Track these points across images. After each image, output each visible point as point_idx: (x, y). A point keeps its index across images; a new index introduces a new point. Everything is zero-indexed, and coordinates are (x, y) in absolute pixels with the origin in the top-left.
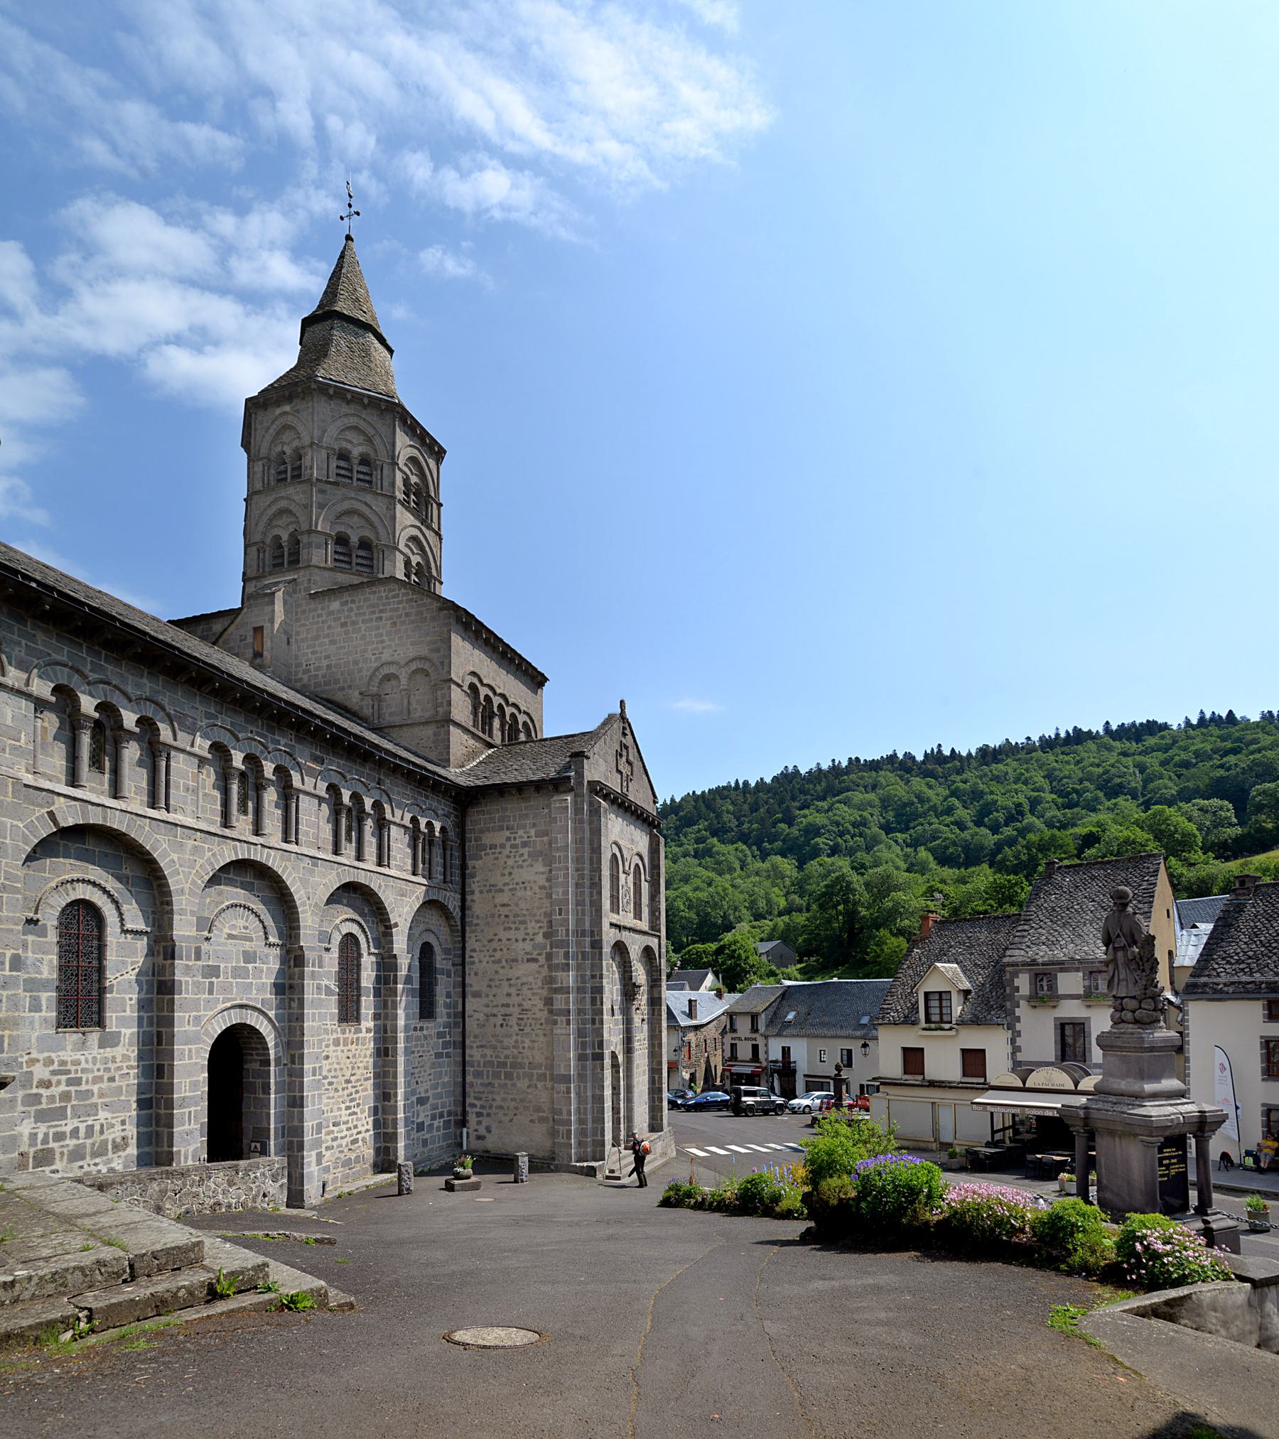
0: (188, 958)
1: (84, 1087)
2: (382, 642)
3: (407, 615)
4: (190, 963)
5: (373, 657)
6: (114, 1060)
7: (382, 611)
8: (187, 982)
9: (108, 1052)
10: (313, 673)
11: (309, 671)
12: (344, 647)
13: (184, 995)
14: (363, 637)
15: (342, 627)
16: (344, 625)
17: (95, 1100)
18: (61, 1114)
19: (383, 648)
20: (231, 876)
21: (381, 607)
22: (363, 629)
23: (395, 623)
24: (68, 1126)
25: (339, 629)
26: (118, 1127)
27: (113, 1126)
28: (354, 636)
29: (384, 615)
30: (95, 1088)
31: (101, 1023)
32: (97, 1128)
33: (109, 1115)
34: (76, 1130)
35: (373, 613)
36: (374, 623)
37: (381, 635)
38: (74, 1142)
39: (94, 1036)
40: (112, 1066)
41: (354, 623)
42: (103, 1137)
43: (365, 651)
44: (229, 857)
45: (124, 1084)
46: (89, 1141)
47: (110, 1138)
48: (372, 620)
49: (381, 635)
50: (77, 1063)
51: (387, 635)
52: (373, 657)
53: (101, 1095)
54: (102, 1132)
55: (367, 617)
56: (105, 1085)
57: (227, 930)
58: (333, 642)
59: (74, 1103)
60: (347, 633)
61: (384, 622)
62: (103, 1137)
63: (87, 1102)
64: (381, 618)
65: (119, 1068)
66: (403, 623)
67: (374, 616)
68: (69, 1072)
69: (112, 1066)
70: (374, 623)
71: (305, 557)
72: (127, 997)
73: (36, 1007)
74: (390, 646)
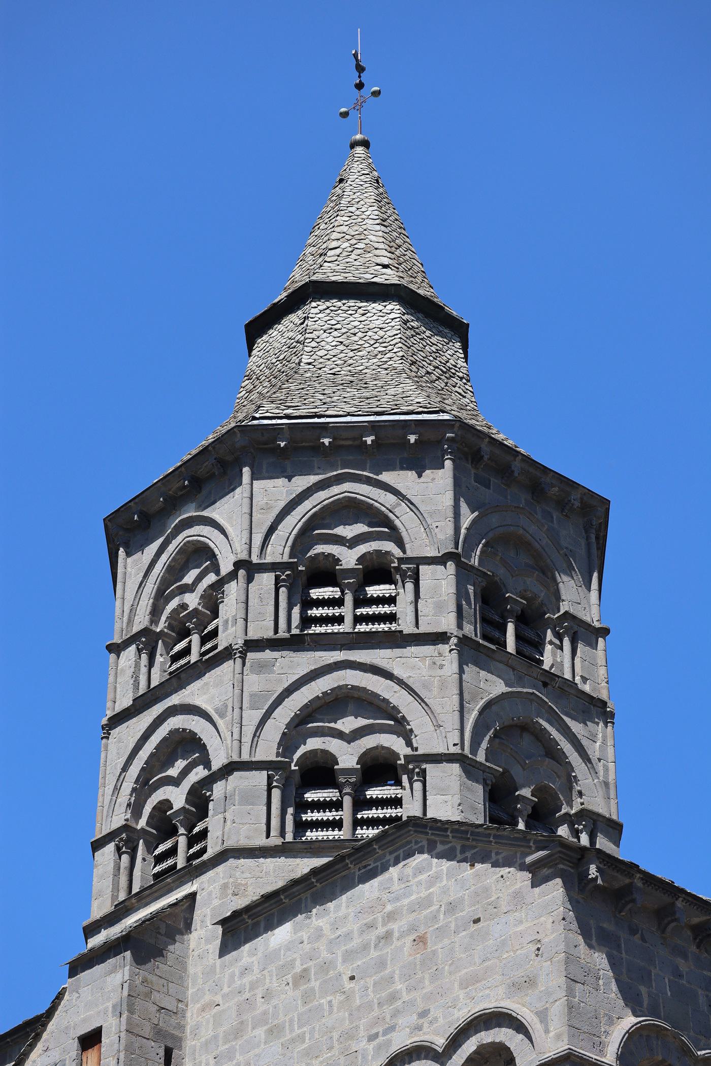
3: (452, 907)
5: (371, 1047)
7: (391, 917)
12: (301, 1038)
14: (348, 997)
15: (296, 984)
19: (396, 1013)
21: (389, 908)
23: (421, 940)
25: (290, 992)
29: (395, 926)
35: (371, 926)
36: (374, 954)
37: (390, 979)
41: (325, 967)
43: (349, 1035)
48: (365, 947)
52: (371, 1047)
55: (356, 942)
58: (274, 1032)
61: (396, 943)
66: (442, 932)
67: (372, 936)
70: (374, 954)
74: (412, 1003)
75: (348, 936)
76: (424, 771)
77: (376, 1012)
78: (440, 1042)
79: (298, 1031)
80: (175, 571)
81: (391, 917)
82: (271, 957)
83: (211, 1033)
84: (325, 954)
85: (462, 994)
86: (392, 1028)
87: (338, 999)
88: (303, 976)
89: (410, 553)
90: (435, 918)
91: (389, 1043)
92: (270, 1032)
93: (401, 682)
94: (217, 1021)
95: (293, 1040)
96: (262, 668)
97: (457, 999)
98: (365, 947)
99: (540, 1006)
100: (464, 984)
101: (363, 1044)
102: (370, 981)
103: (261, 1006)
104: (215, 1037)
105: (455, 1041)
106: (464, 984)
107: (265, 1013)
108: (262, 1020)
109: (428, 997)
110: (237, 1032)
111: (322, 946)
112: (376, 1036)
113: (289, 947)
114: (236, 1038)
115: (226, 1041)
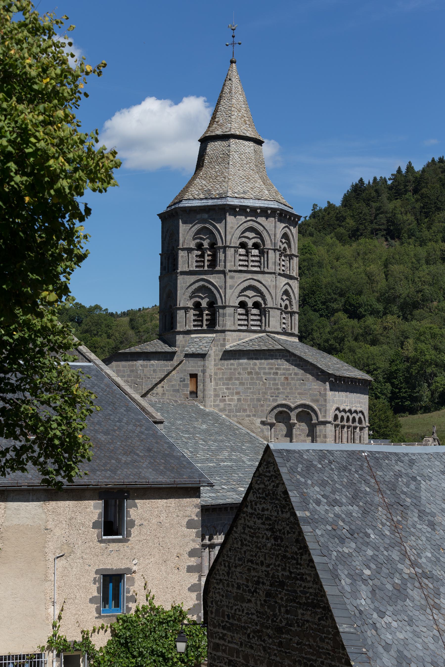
2: (278, 389)
7: (277, 369)
10: (228, 403)
11: (225, 400)
12: (250, 389)
16: (250, 373)
19: (279, 393)
21: (277, 366)
22: (264, 378)
25: (247, 376)
28: (258, 382)
29: (279, 372)
35: (272, 369)
37: (277, 384)
41: (257, 373)
43: (265, 393)
48: (270, 373)
49: (277, 384)
51: (281, 385)
52: (271, 398)
55: (267, 371)
58: (242, 384)
60: (252, 379)
64: (276, 374)
66: (293, 379)
67: (272, 371)
70: (272, 376)
71: (221, 323)
75: (265, 368)
76: (269, 311)
77: (273, 391)
78: (293, 406)
79: (249, 386)
80: (198, 232)
81: (277, 369)
82: (241, 364)
83: (221, 376)
84: (257, 370)
85: (298, 396)
86: (278, 396)
87: (261, 383)
88: (250, 373)
89: (266, 247)
90: (291, 374)
91: (276, 400)
92: (240, 383)
93: (264, 285)
94: (223, 374)
95: (248, 388)
96: (232, 278)
97: (296, 397)
98: (270, 373)
99: (320, 407)
100: (299, 394)
101: (269, 397)
102: (272, 382)
103: (237, 376)
104: (223, 378)
105: (297, 407)
106: (299, 394)
107: (239, 378)
108: (238, 379)
109: (288, 393)
110: (230, 379)
111: (257, 368)
112: (273, 396)
113: (246, 364)
114: (229, 380)
115: (226, 380)
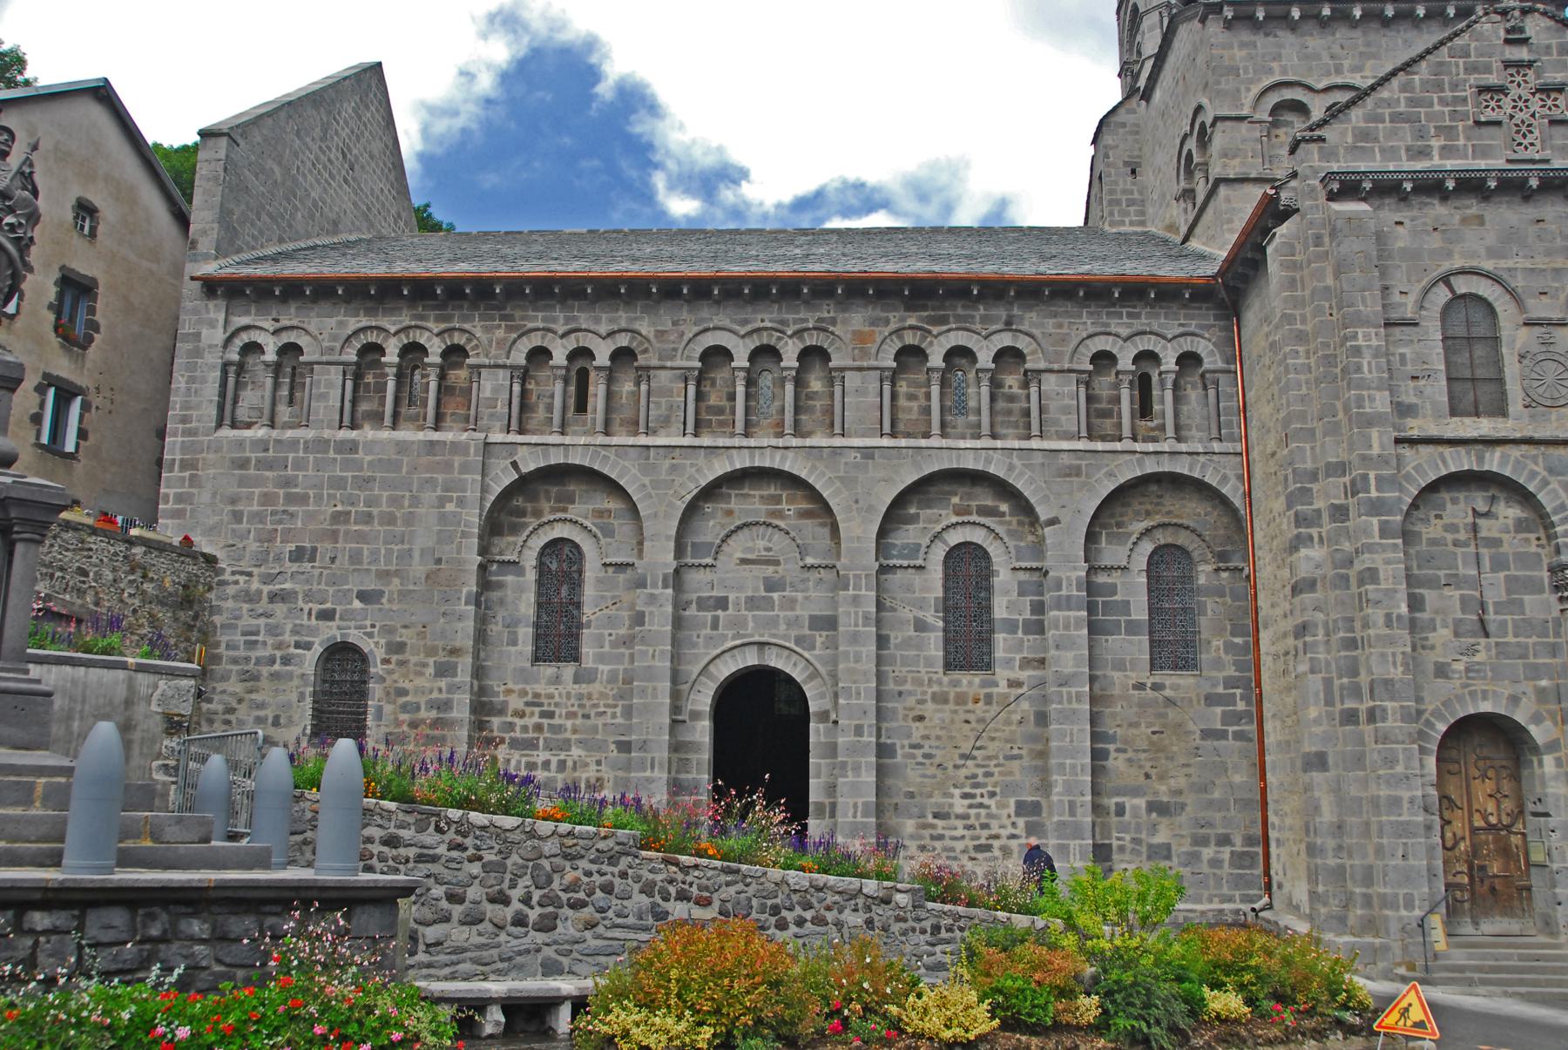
0: (654, 586)
1: (556, 721)
4: (656, 592)
6: (590, 696)
8: (651, 613)
9: (584, 688)
13: (647, 627)
17: (568, 735)
18: (531, 745)
20: (746, 491)
24: (541, 756)
26: (594, 767)
27: (586, 765)
30: (569, 723)
31: (576, 658)
32: (570, 764)
33: (583, 753)
34: (546, 764)
38: (546, 774)
39: (568, 670)
40: (588, 703)
42: (577, 774)
44: (720, 467)
45: (600, 722)
46: (560, 776)
47: (584, 776)
50: (551, 696)
53: (575, 731)
54: (574, 768)
56: (579, 721)
57: (740, 555)
59: (547, 735)
62: (577, 774)
63: (559, 737)
65: (595, 706)
68: (540, 705)
69: (588, 703)
72: (606, 632)
73: (514, 643)
